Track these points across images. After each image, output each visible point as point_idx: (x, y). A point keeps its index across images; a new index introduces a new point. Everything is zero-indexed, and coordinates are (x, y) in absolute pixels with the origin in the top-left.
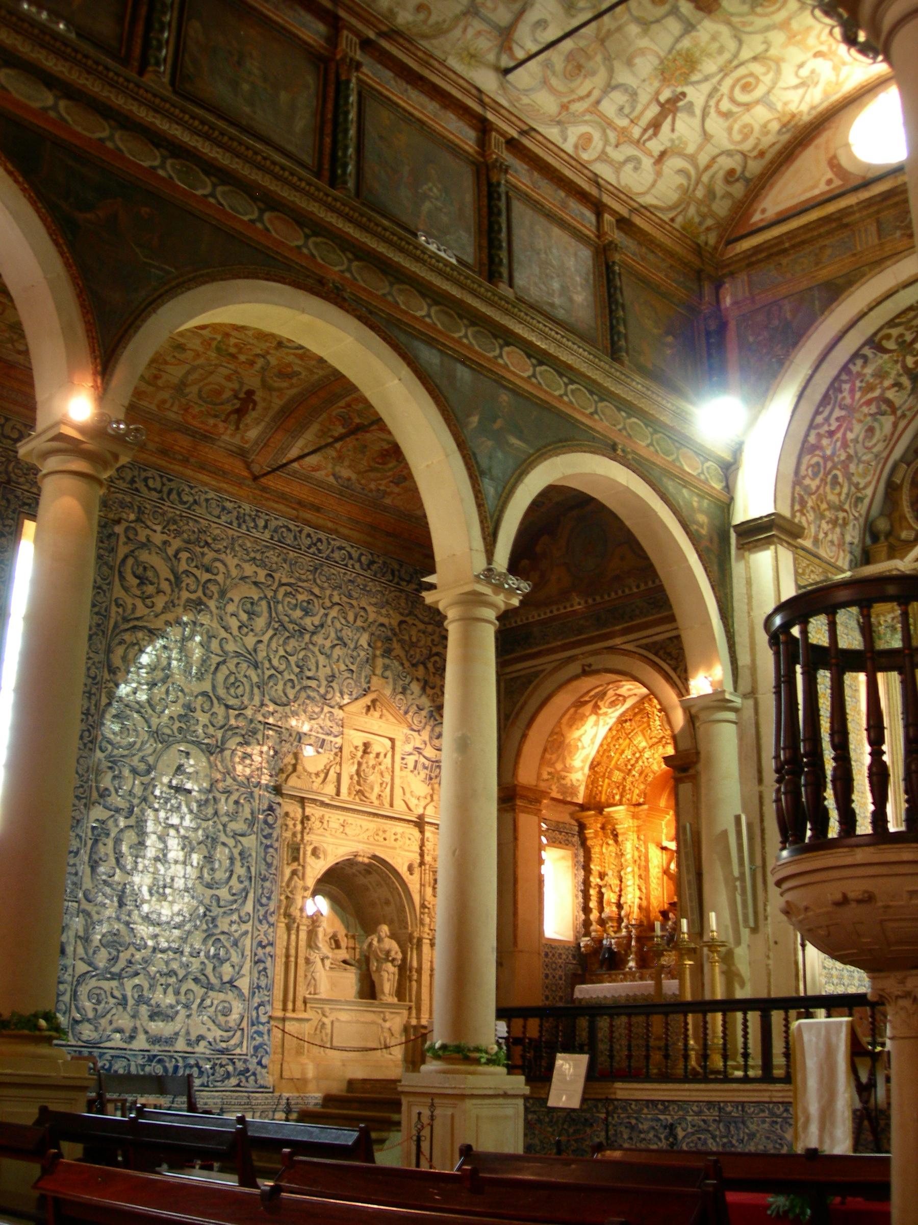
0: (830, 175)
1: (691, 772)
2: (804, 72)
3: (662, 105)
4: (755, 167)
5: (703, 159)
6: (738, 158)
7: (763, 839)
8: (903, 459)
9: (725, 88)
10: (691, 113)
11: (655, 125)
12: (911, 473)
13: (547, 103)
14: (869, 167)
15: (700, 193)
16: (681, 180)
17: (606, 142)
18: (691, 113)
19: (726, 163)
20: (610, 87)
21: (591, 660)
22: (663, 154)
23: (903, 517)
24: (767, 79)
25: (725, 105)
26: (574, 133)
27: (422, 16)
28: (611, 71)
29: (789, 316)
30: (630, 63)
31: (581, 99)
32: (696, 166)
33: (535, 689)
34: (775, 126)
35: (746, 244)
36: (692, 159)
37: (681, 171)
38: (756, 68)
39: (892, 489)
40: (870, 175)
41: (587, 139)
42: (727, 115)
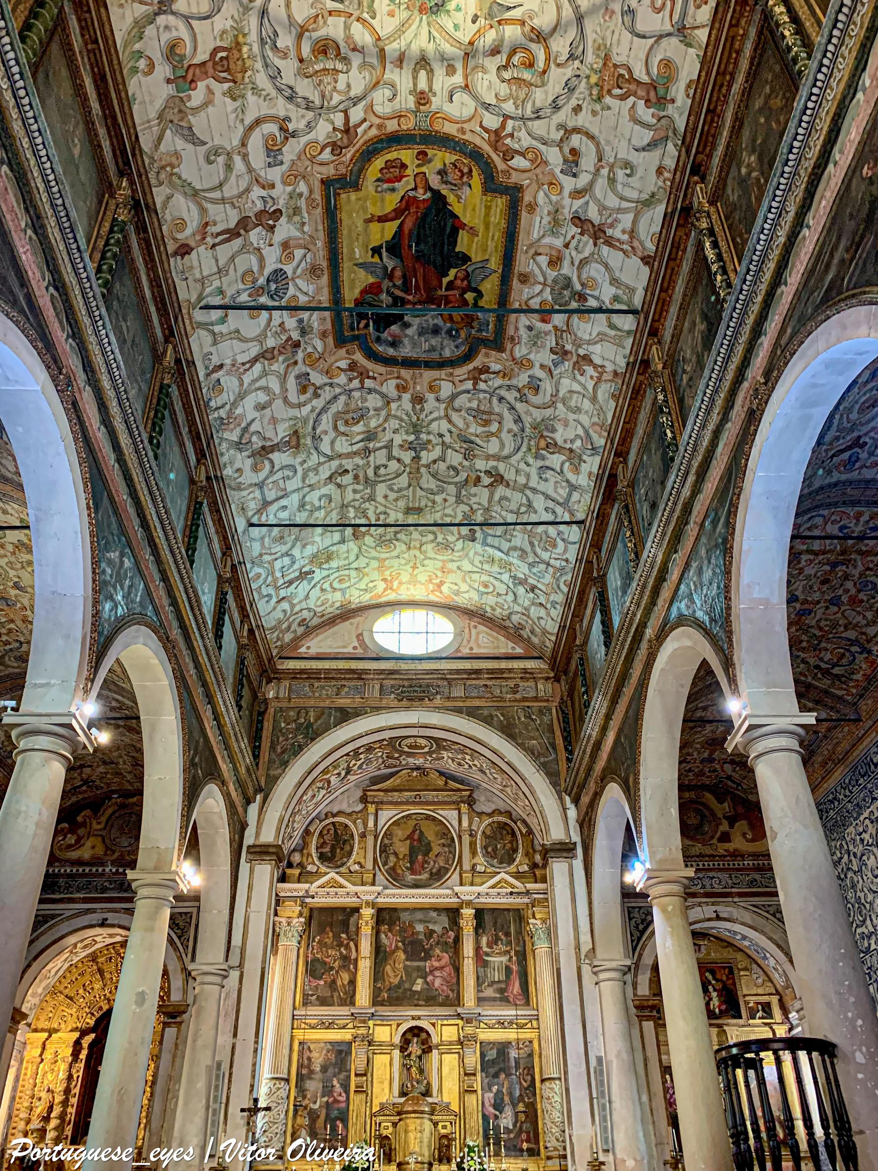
0: (356, 644)
1: (178, 1019)
2: (371, 585)
3: (301, 573)
4: (315, 621)
5: (297, 609)
6: (312, 614)
7: (230, 1081)
8: (317, 817)
9: (332, 578)
10: (309, 583)
11: (291, 582)
12: (320, 827)
13: (256, 548)
14: (382, 649)
15: (284, 626)
16: (281, 616)
17: (265, 581)
18: (309, 583)
19: (306, 614)
20: (287, 554)
21: (109, 915)
22: (284, 598)
23: (309, 855)
24: (353, 581)
25: (326, 586)
26: (257, 570)
27: (236, 475)
28: (293, 546)
29: (312, 720)
30: (304, 546)
31: (271, 554)
32: (292, 610)
33: (50, 928)
34: (338, 604)
35: (292, 665)
36: (293, 606)
37: (284, 611)
38: (353, 573)
39: (307, 832)
40: (382, 655)
41: (258, 576)
42: (322, 590)
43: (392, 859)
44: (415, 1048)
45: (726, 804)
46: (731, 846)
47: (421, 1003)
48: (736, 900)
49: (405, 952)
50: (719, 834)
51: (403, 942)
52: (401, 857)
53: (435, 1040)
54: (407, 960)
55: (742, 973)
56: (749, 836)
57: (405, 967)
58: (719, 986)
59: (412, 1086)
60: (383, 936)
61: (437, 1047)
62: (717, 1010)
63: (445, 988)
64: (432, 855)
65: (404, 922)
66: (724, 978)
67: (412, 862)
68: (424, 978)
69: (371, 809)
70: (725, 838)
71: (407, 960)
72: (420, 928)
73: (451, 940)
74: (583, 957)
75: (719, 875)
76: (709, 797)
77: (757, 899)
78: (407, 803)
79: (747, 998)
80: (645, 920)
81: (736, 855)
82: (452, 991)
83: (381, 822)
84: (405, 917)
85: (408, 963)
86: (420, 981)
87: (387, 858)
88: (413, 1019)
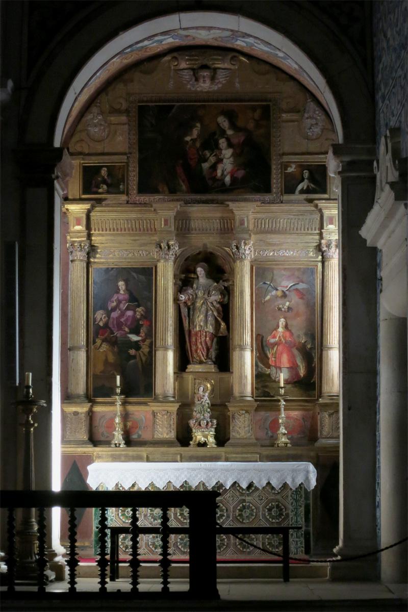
58: (239, 138)
62: (228, 179)
66: (251, 125)
79: (286, 159)
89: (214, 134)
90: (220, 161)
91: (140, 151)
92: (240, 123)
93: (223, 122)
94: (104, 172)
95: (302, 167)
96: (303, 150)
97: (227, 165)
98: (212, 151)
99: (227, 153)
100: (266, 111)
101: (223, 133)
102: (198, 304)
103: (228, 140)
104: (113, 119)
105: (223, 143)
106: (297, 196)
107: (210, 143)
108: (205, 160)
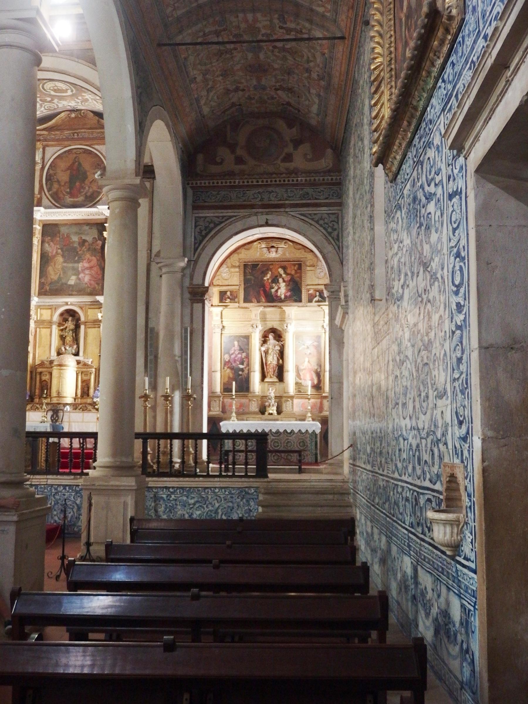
43: (56, 186)
44: (70, 325)
45: (294, 129)
46: (292, 165)
47: (74, 293)
48: (287, 210)
49: (63, 256)
50: (284, 155)
51: (62, 249)
52: (63, 184)
53: (83, 319)
54: (64, 262)
55: (308, 268)
56: (308, 157)
57: (63, 268)
58: (287, 278)
59: (66, 349)
60: (47, 245)
61: (85, 323)
62: (283, 297)
63: (92, 282)
64: (86, 182)
65: (63, 235)
66: (293, 272)
67: (71, 188)
68: (77, 273)
69: (39, 145)
70: (288, 158)
71: (65, 262)
72: (75, 239)
73: (99, 247)
74: (153, 256)
75: (277, 190)
76: (281, 125)
77: (305, 209)
78: (67, 139)
80: (208, 226)
81: (295, 172)
82: (98, 284)
83: (47, 156)
84: (64, 230)
85: (65, 264)
86: (74, 278)
87: (52, 185)
88: (67, 304)
89: (277, 276)
90: (279, 288)
91: (245, 284)
92: (289, 271)
93: (281, 271)
94: (228, 293)
95: (316, 291)
96: (316, 283)
97: (282, 290)
98: (276, 283)
99: (283, 285)
100: (299, 266)
101: (281, 275)
102: (270, 352)
103: (283, 279)
104: (233, 270)
105: (281, 280)
106: (313, 304)
107: (275, 280)
108: (273, 288)
